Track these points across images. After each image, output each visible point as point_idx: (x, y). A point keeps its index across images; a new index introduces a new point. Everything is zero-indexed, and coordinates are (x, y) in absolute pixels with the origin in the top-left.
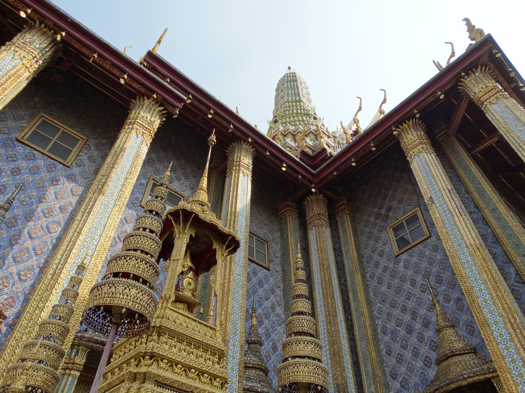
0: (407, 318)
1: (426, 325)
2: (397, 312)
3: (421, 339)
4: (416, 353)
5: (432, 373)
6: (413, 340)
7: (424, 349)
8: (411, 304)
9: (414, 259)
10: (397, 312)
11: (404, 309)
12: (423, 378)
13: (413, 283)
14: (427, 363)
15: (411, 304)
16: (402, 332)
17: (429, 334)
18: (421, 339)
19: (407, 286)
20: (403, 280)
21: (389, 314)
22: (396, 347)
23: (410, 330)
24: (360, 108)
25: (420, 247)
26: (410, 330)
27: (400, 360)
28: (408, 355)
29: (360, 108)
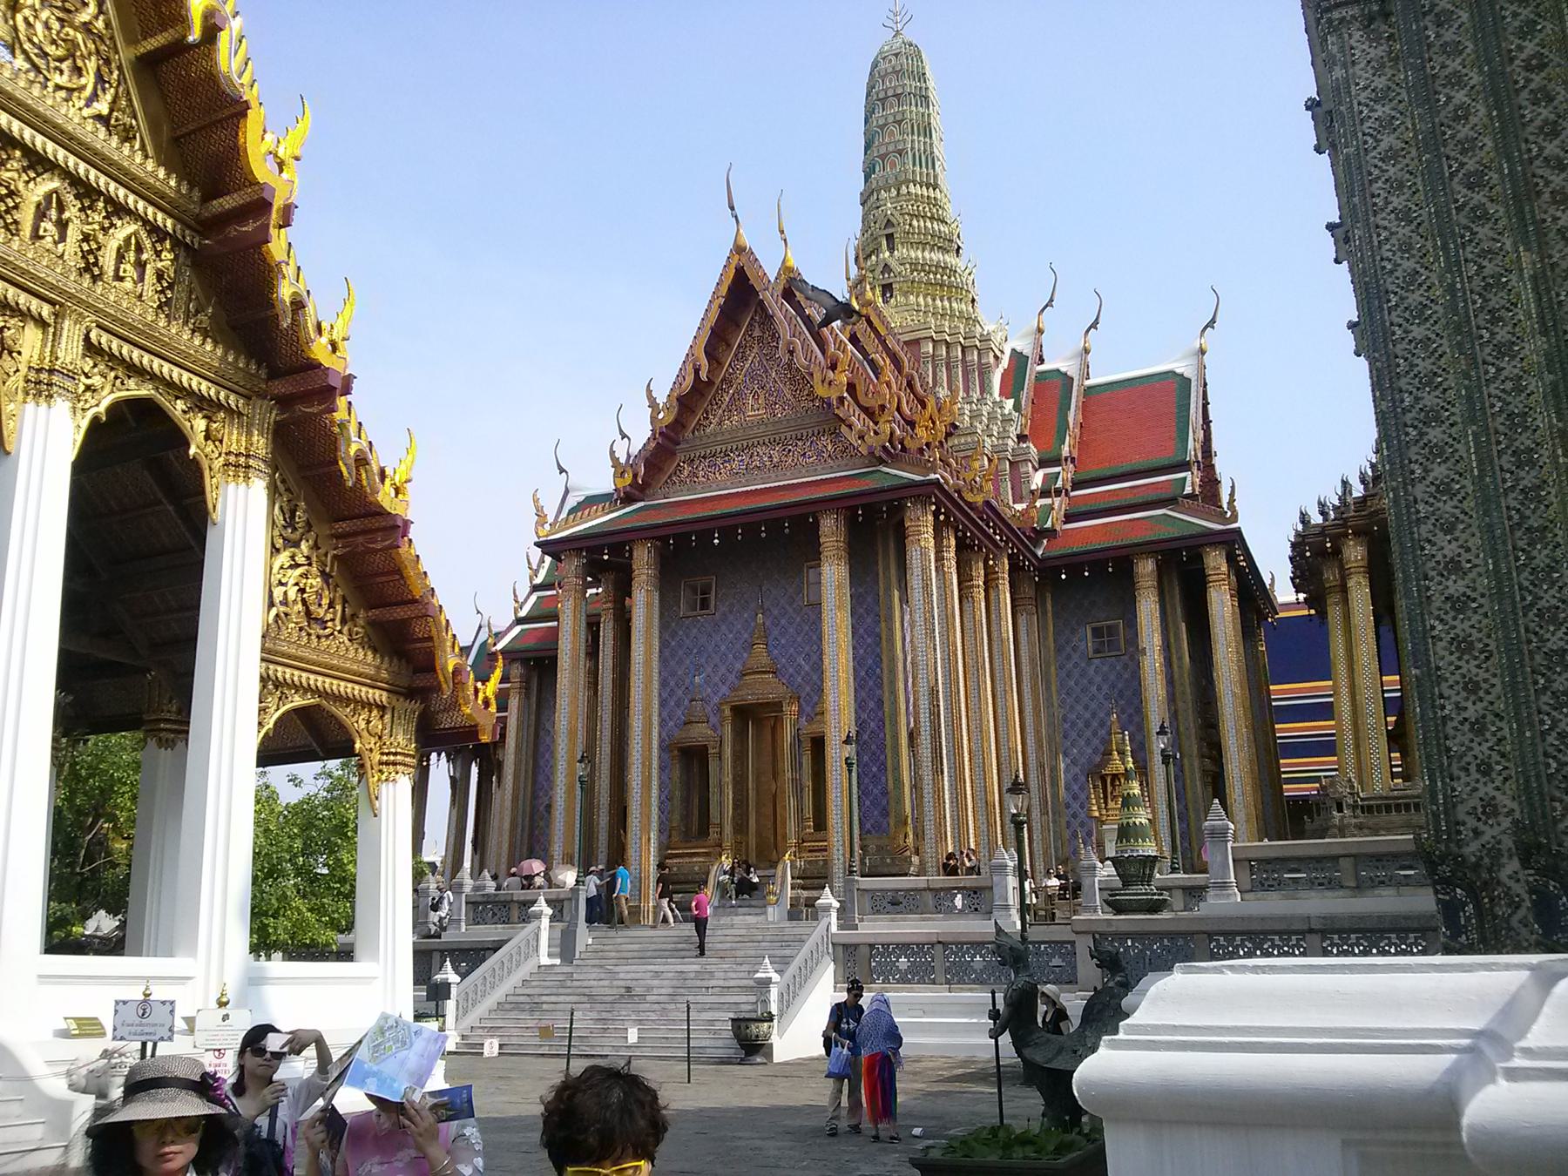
0: (1087, 715)
2: (1079, 708)
3: (1095, 734)
4: (1088, 742)
6: (1088, 733)
7: (1096, 742)
8: (1093, 705)
9: (1105, 668)
10: (1079, 708)
11: (1086, 708)
12: (1090, 761)
14: (1095, 751)
15: (1093, 705)
16: (1080, 724)
17: (1102, 732)
18: (1095, 734)
19: (1094, 689)
22: (1074, 735)
24: (1051, 300)
29: (1051, 300)
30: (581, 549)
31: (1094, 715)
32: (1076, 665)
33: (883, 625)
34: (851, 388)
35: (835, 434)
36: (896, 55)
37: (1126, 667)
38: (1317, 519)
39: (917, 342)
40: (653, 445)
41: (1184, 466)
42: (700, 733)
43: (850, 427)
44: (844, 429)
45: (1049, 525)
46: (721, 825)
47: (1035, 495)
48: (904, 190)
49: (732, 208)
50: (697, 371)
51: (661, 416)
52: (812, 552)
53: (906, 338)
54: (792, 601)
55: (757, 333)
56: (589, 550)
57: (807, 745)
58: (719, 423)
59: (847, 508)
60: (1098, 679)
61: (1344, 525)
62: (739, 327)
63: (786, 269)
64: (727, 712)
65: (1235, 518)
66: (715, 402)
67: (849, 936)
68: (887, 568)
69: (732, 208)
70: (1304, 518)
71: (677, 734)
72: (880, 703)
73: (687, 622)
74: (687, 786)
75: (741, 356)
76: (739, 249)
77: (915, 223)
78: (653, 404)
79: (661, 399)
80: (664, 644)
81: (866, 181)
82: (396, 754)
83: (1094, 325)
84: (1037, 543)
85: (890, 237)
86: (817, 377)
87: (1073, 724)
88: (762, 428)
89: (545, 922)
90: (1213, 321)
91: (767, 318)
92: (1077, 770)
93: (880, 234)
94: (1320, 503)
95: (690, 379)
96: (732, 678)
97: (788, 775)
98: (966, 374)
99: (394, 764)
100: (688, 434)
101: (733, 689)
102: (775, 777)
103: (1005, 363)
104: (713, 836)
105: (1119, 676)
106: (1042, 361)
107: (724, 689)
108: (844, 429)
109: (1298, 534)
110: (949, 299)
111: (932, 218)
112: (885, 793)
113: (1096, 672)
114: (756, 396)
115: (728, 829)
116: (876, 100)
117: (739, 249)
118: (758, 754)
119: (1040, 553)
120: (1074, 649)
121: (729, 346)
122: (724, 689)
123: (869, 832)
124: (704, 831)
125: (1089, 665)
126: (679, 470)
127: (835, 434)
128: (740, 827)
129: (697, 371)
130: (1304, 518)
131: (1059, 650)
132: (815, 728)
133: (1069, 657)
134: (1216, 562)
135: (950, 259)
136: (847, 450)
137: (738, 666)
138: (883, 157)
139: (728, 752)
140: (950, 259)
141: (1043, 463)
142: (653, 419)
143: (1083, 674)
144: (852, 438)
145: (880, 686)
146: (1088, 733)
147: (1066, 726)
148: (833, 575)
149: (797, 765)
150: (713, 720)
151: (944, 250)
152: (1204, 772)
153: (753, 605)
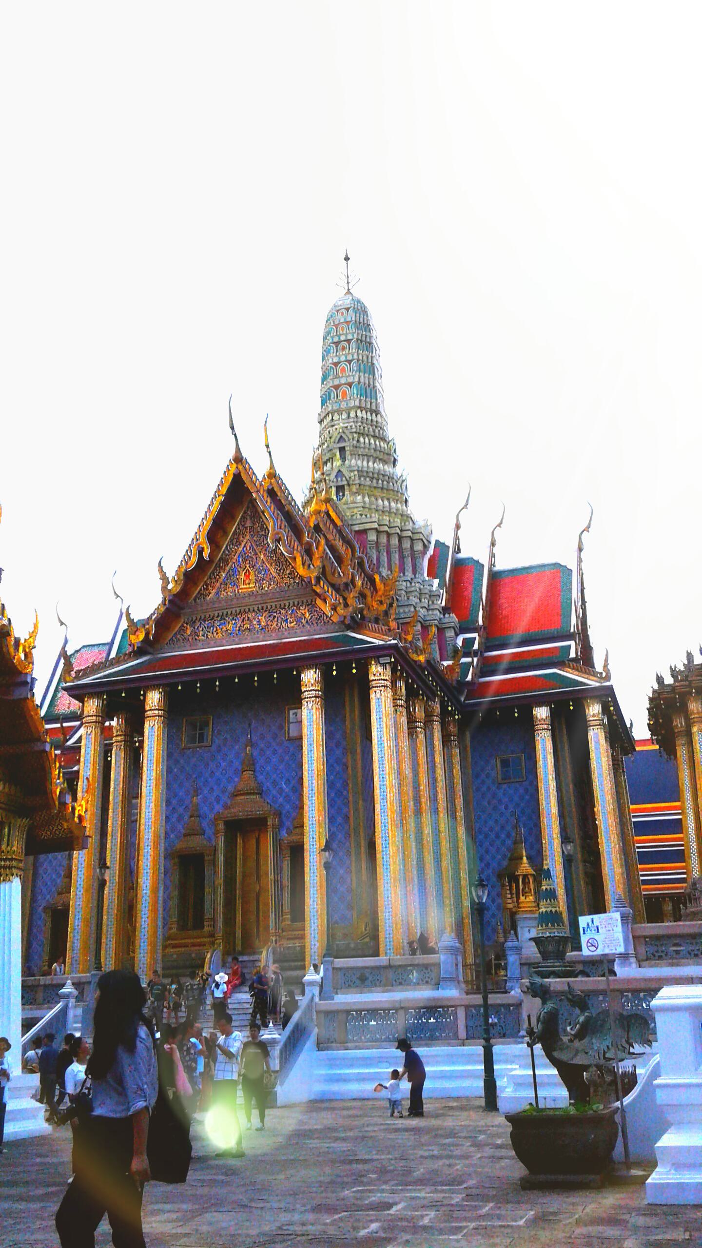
0: (497, 829)
1: (508, 836)
3: (503, 843)
5: (505, 863)
6: (498, 843)
7: (504, 849)
9: (511, 792)
10: (491, 823)
13: (506, 808)
17: (509, 842)
18: (503, 843)
20: (500, 801)
21: (486, 822)
23: (497, 836)
25: (517, 785)
26: (497, 836)
27: (487, 852)
28: (493, 850)
30: (102, 693)
31: (503, 827)
32: (489, 788)
33: (349, 757)
34: (324, 572)
35: (312, 605)
36: (348, 309)
37: (526, 791)
38: (669, 680)
39: (365, 532)
40: (162, 609)
41: (570, 637)
42: (196, 843)
43: (325, 601)
44: (319, 602)
45: (469, 678)
46: (214, 920)
47: (459, 653)
48: (352, 414)
49: (232, 428)
50: (201, 552)
51: (170, 587)
52: (296, 700)
53: (357, 528)
54: (275, 736)
55: (248, 524)
56: (108, 693)
57: (287, 853)
58: (218, 593)
59: (324, 664)
60: (505, 800)
61: (690, 686)
62: (233, 518)
63: (272, 474)
64: (221, 826)
65: (608, 678)
66: (214, 577)
67: (325, 1005)
68: (352, 711)
69: (232, 428)
70: (660, 680)
71: (179, 845)
72: (347, 818)
73: (188, 752)
74: (183, 887)
75: (236, 540)
76: (238, 459)
77: (362, 440)
78: (164, 577)
79: (171, 573)
80: (169, 770)
81: (323, 405)
82: (12, 859)
83: (499, 525)
84: (461, 693)
85: (342, 450)
86: (299, 560)
87: (486, 836)
88: (252, 599)
89: (72, 1001)
90: (589, 527)
91: (256, 514)
92: (490, 871)
93: (335, 448)
94: (671, 668)
95: (194, 560)
96: (225, 798)
97: (271, 877)
98: (402, 557)
99: (10, 868)
100: (191, 600)
101: (226, 807)
102: (258, 878)
103: (431, 551)
104: (206, 929)
105: (522, 798)
106: (459, 551)
107: (218, 808)
108: (319, 602)
109: (654, 691)
110: (388, 499)
111: (374, 436)
112: (349, 890)
113: (504, 794)
114: (247, 576)
115: (220, 923)
116: (334, 342)
117: (238, 459)
118: (245, 859)
119: (462, 699)
120: (488, 776)
121: (226, 533)
122: (218, 808)
123: (336, 922)
124: (199, 924)
125: (498, 788)
126: (182, 630)
127: (312, 605)
128: (229, 921)
129: (201, 552)
130: (660, 680)
131: (477, 776)
132: (295, 838)
133: (483, 782)
134: (594, 710)
135: (388, 469)
136: (321, 617)
137: (230, 788)
138: (337, 387)
139: (221, 859)
140: (388, 469)
141: (463, 630)
142: (164, 589)
143: (494, 795)
144: (327, 610)
145: (347, 804)
146: (498, 843)
147: (481, 837)
148: (311, 718)
149: (278, 870)
150: (209, 832)
151: (385, 462)
152: (586, 874)
153: (243, 740)
